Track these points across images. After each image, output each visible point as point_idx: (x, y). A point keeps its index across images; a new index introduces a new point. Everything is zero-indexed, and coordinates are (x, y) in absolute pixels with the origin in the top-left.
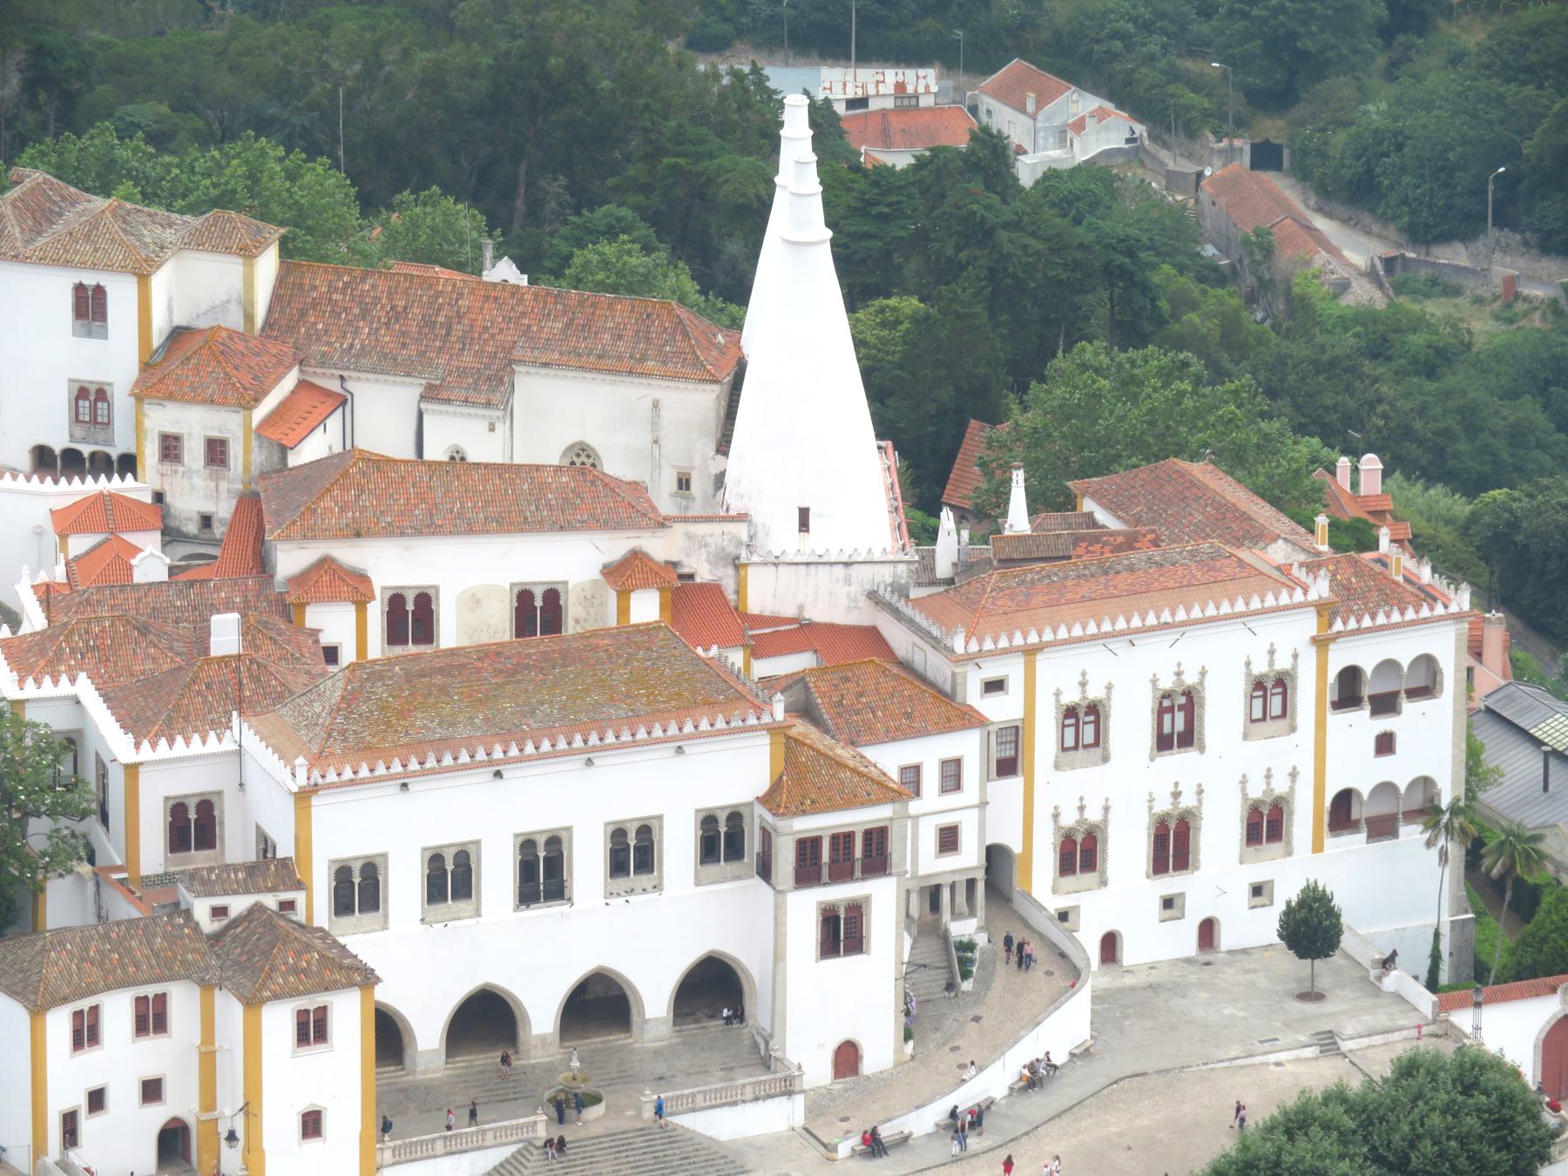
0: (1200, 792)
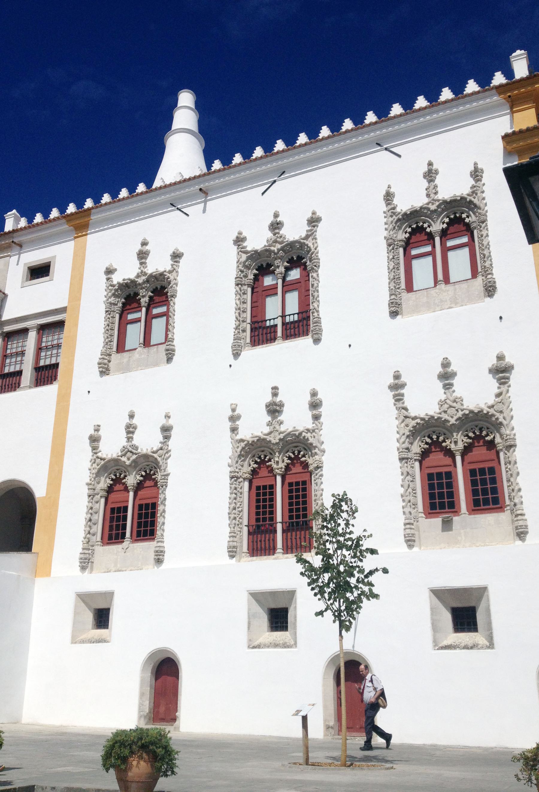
0: (315, 405)
